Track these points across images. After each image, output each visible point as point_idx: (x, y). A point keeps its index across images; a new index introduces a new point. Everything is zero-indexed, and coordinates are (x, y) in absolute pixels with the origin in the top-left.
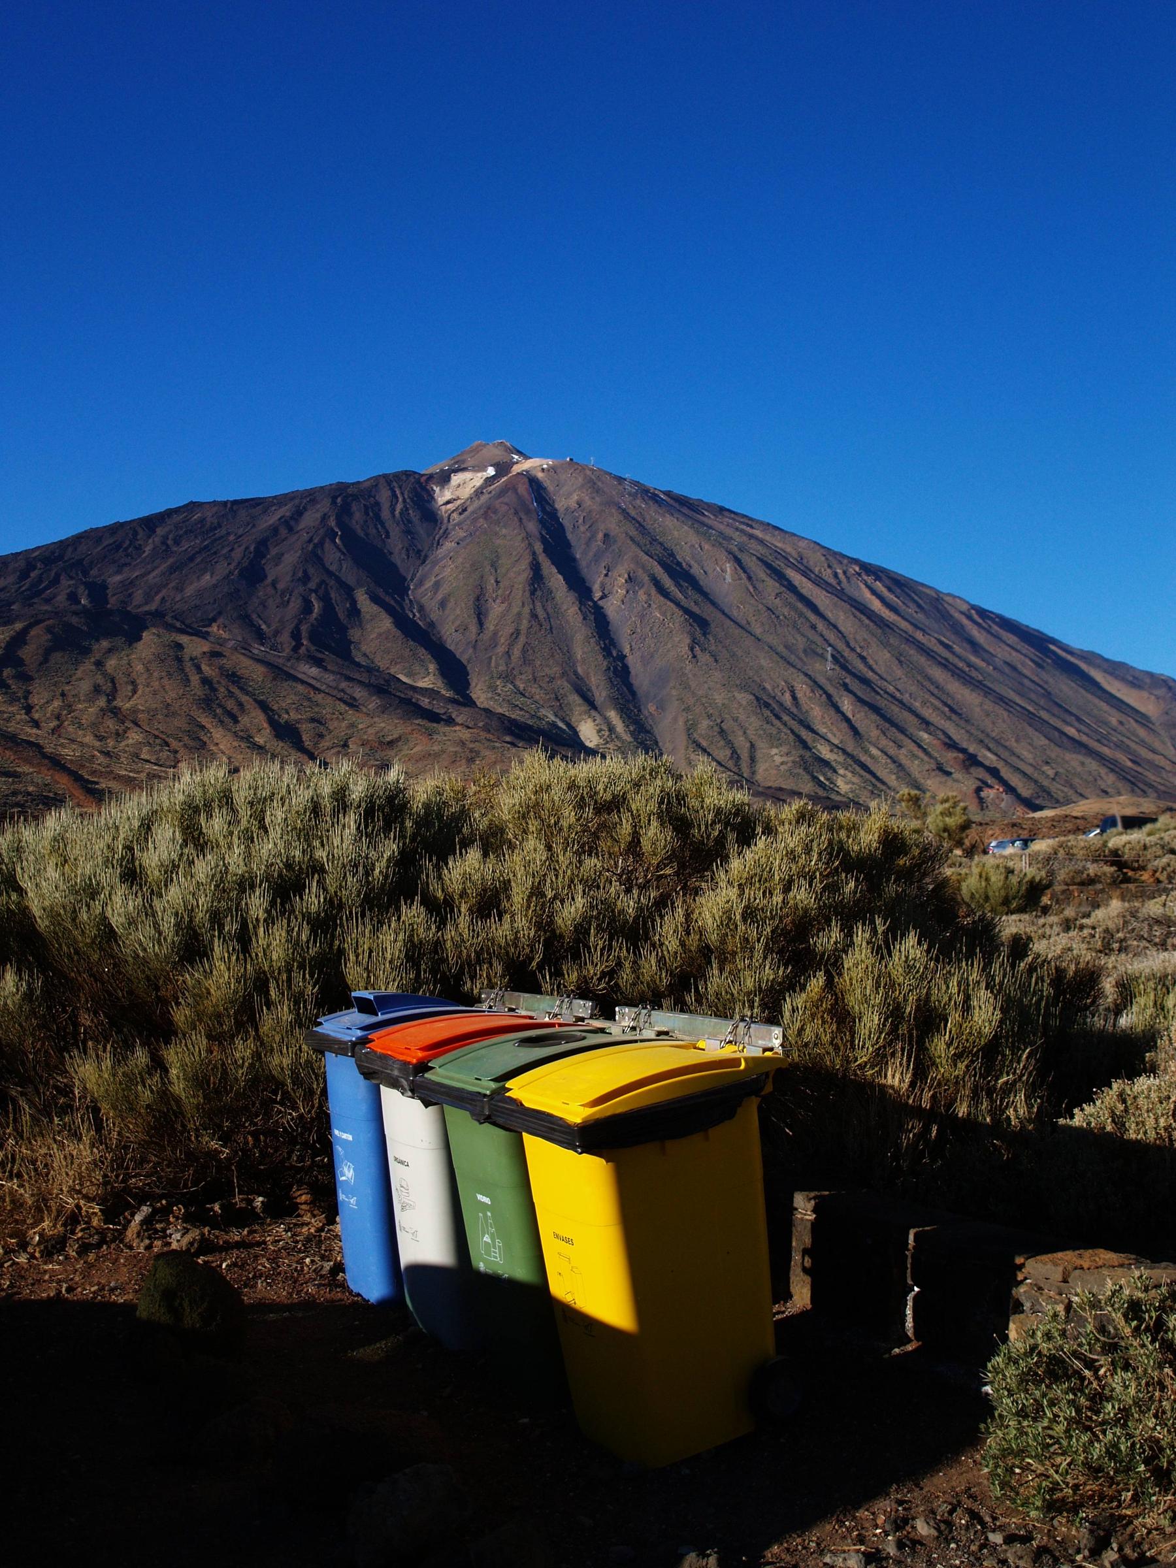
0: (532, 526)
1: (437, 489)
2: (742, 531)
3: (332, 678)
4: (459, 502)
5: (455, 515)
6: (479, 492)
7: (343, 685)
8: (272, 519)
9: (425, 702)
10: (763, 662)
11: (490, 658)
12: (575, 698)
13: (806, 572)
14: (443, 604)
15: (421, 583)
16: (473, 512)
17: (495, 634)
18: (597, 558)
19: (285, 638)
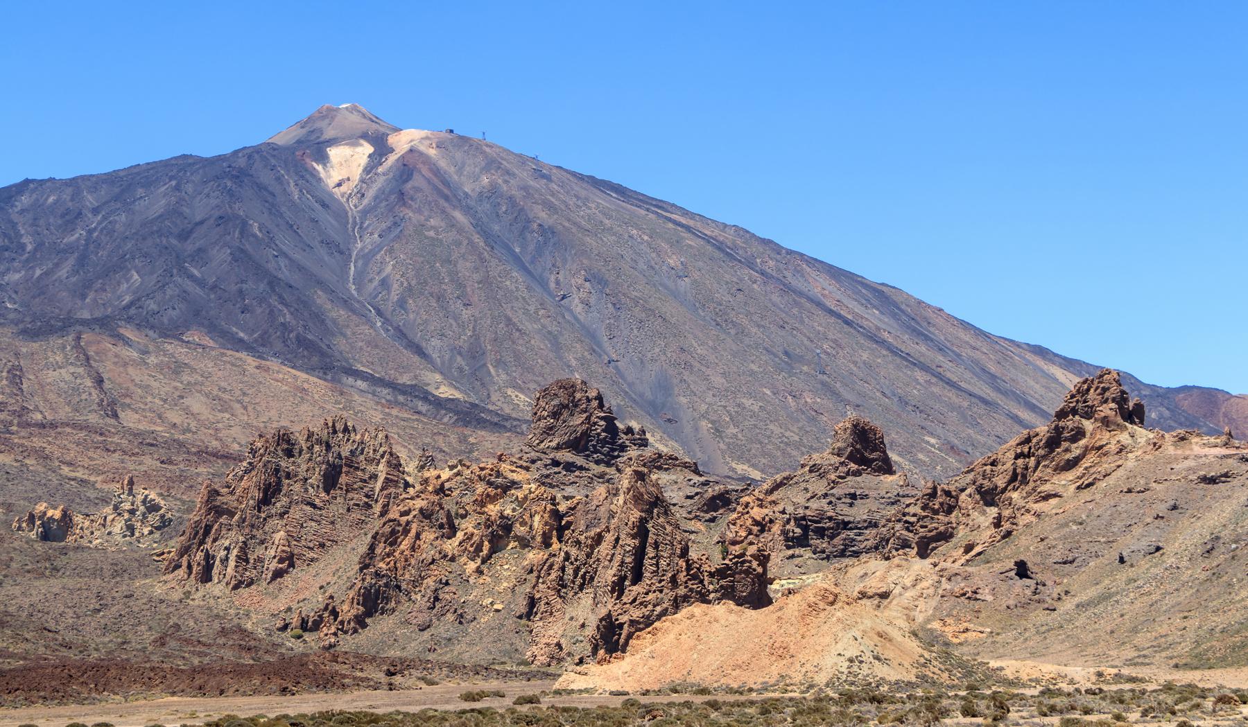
0: (458, 215)
1: (319, 168)
2: (666, 218)
3: (385, 391)
4: (352, 184)
5: (354, 201)
6: (369, 169)
7: (401, 398)
8: (155, 203)
10: (754, 367)
11: (485, 365)
13: (751, 265)
14: (402, 303)
15: (360, 281)
16: (376, 198)
17: (476, 336)
18: (539, 250)
19: (279, 346)
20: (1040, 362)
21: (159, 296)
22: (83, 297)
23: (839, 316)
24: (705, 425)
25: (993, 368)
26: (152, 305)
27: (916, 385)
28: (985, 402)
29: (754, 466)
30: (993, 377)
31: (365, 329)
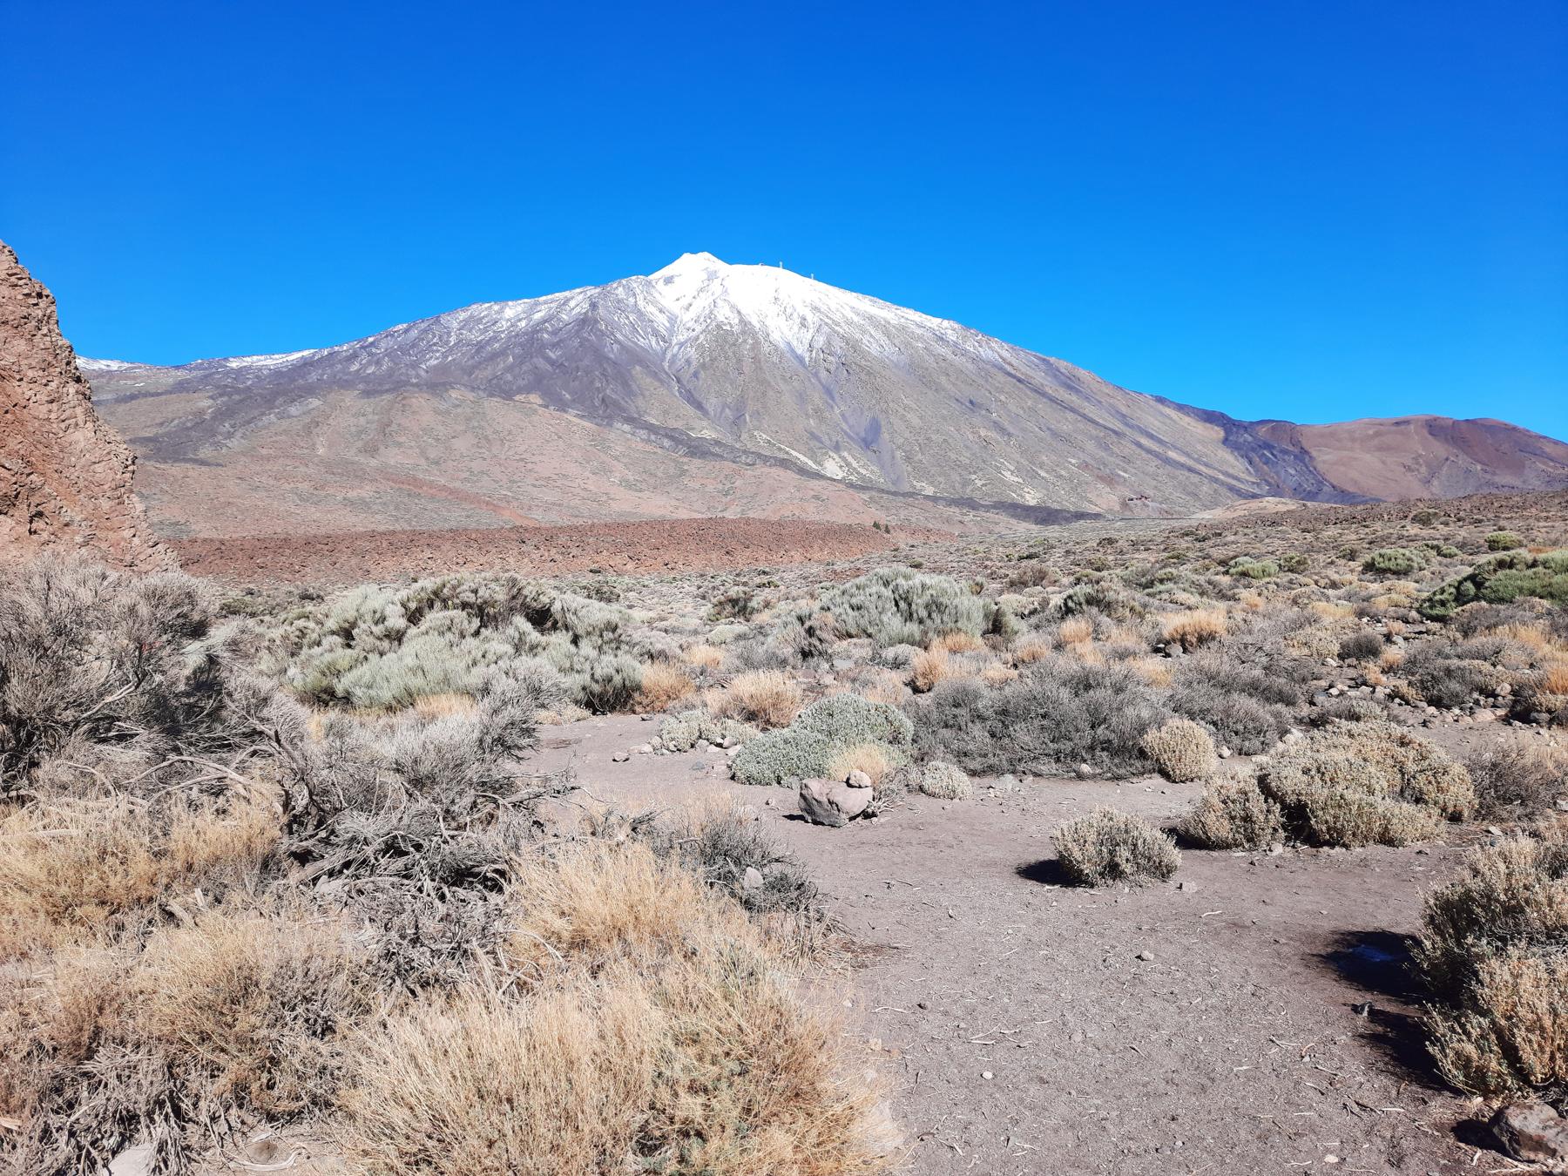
9: (717, 450)
12: (813, 443)
14: (696, 375)
20: (1160, 407)
21: (517, 370)
22: (470, 374)
23: (1014, 377)
24: (899, 454)
25: (1124, 410)
26: (509, 377)
27: (1067, 423)
28: (1115, 432)
29: (932, 483)
30: (1124, 416)
31: (663, 391)
